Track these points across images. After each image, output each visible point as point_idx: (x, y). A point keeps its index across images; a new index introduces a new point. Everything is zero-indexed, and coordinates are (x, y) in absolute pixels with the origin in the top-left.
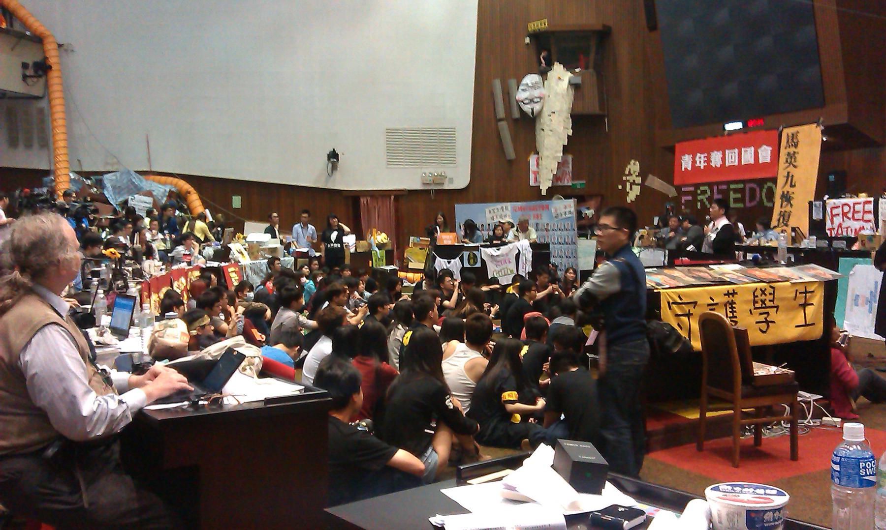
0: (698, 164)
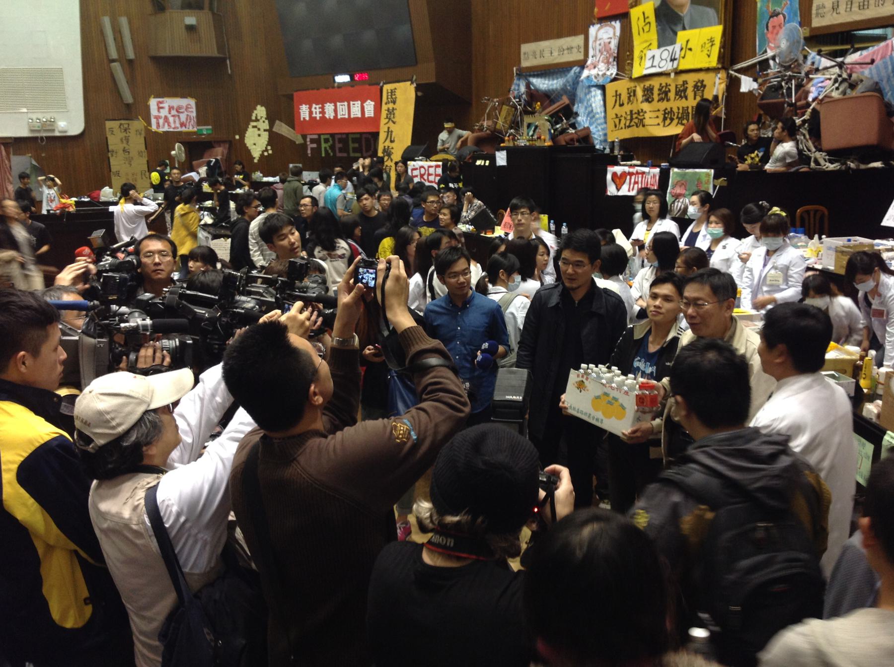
0: (314, 115)
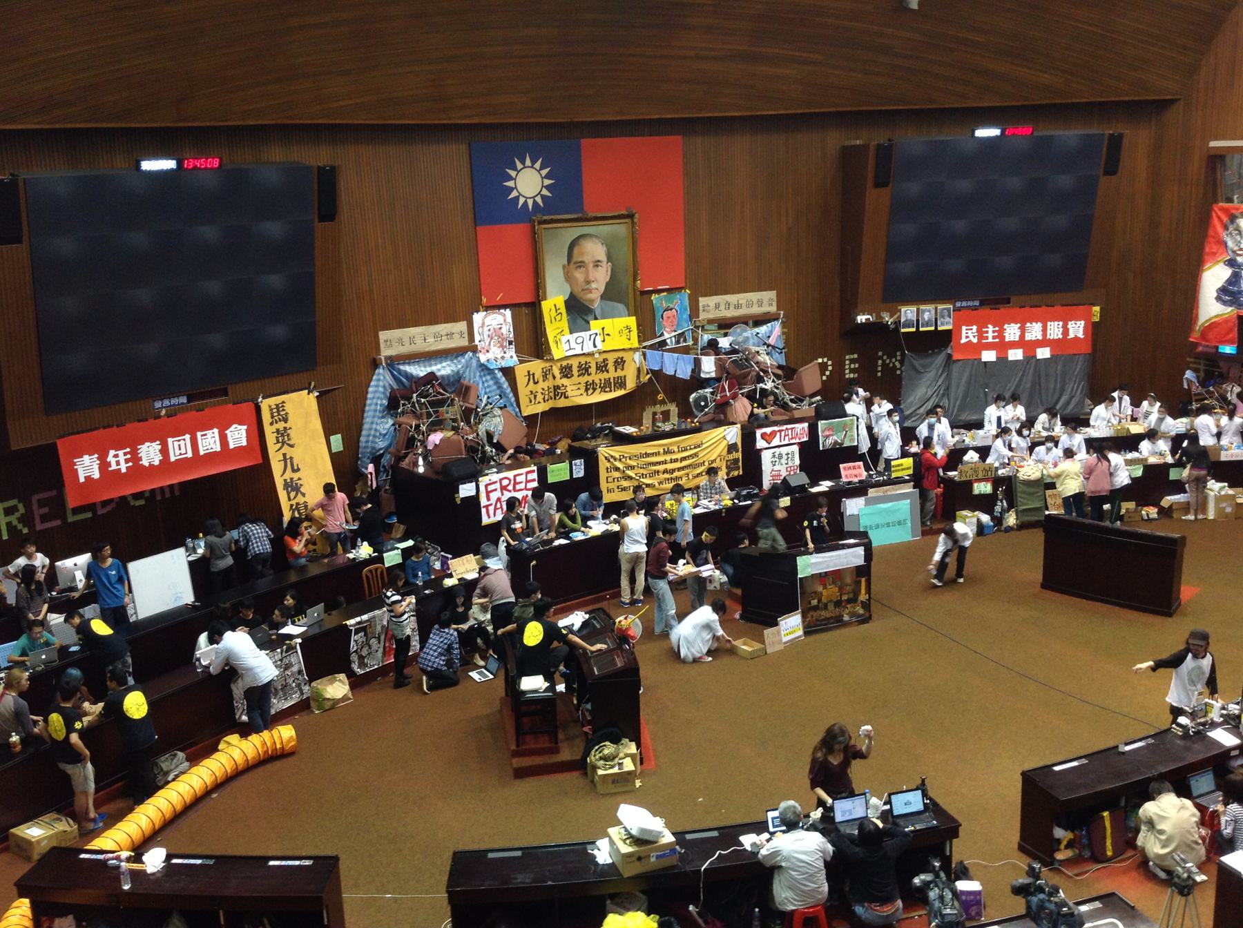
0: (114, 467)
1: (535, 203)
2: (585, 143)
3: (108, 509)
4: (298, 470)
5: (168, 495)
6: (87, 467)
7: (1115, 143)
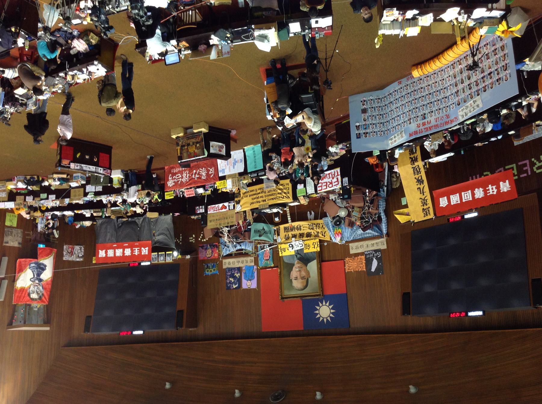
0: (494, 187)
1: (322, 303)
2: (302, 329)
3: (498, 170)
4: (418, 189)
5: (474, 177)
6: (505, 187)
7: (87, 329)
